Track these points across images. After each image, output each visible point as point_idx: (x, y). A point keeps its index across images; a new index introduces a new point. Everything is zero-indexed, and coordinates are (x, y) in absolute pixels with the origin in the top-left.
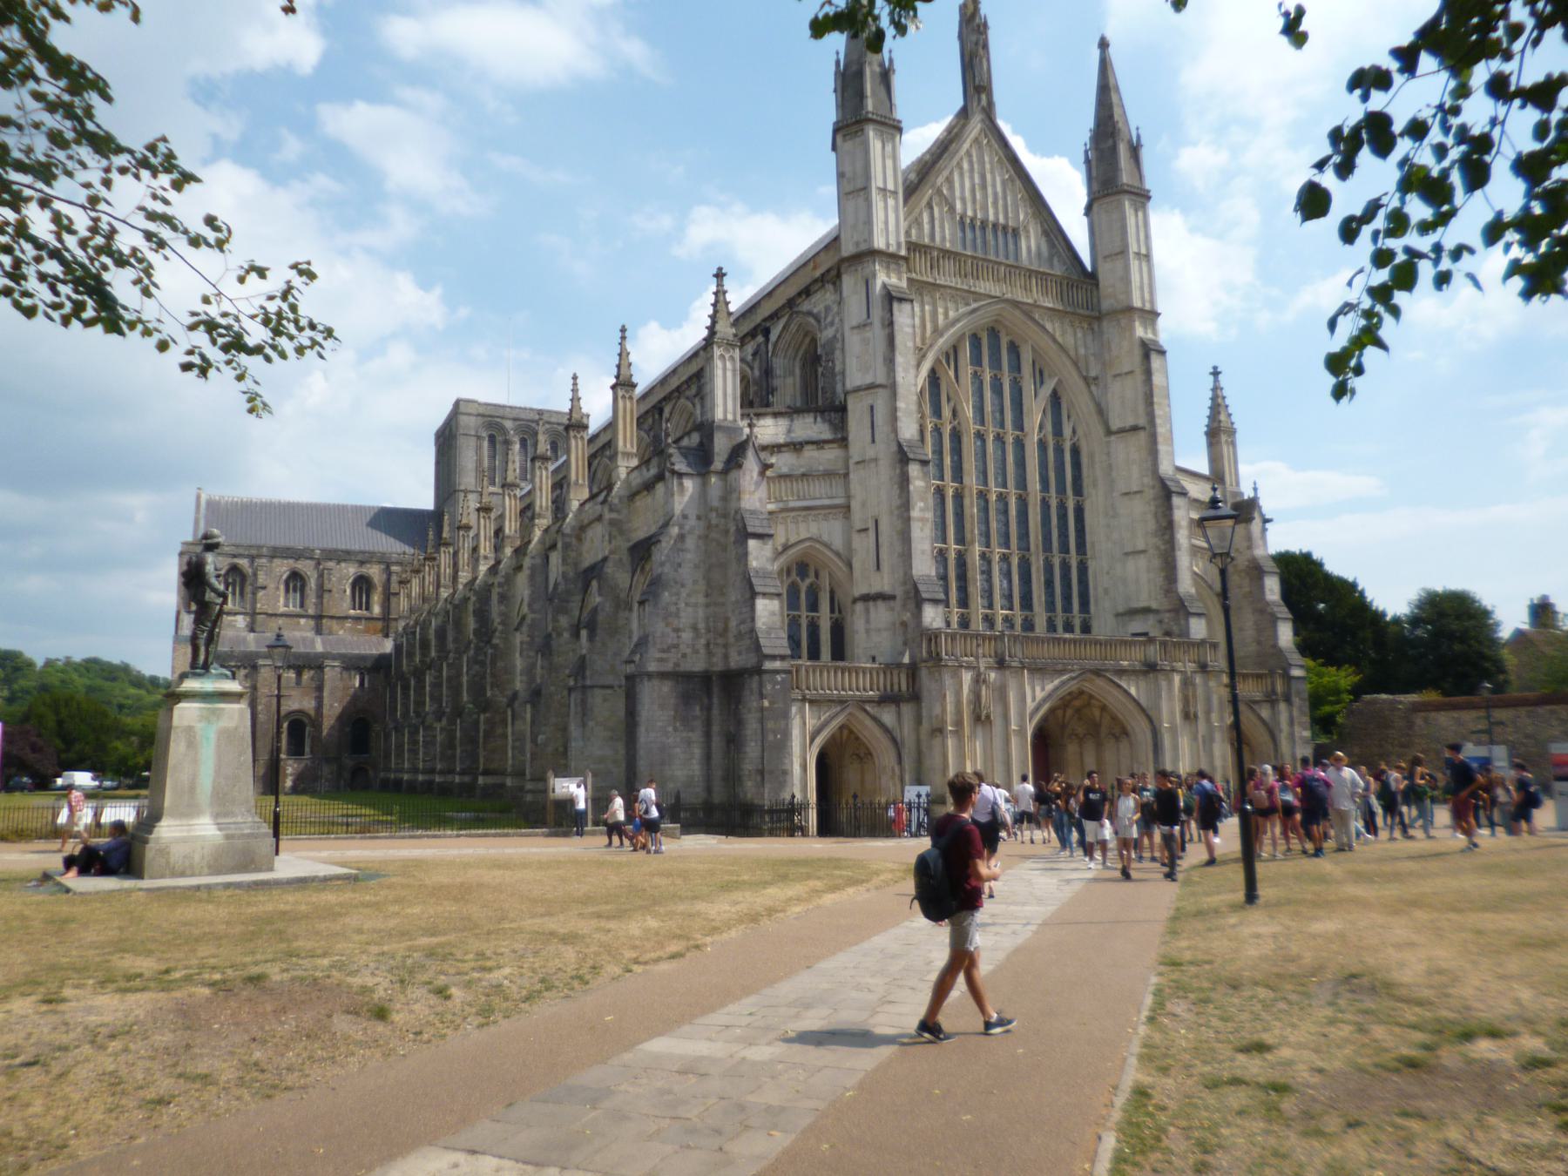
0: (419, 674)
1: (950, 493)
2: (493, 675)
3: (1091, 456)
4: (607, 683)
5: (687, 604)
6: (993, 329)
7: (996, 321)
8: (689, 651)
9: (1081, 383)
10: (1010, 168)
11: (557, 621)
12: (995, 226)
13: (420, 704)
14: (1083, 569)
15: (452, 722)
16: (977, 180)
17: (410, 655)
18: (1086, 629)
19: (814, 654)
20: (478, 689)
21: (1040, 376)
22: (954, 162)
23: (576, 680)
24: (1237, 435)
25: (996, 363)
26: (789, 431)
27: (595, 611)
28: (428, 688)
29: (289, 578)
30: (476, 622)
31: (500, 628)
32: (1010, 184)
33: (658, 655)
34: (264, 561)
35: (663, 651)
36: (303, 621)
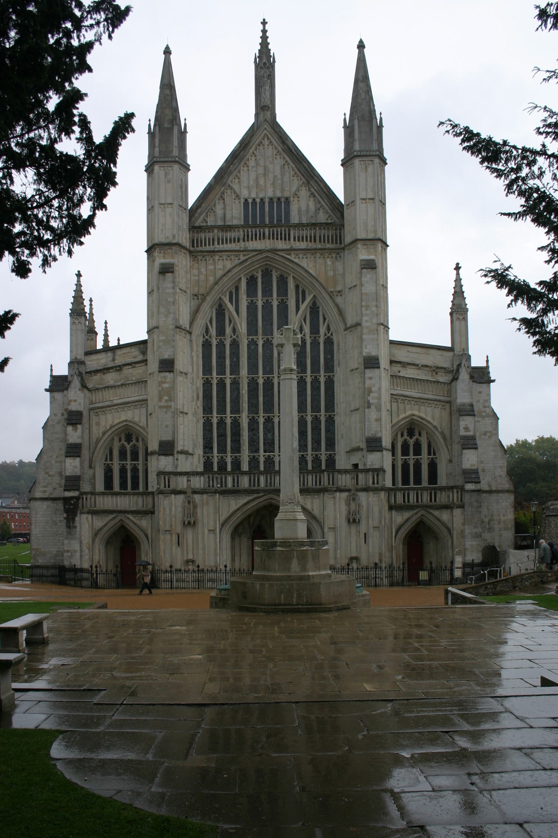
1: (228, 382)
3: (338, 346)
5: (56, 462)
6: (267, 269)
7: (266, 264)
8: (58, 486)
9: (327, 297)
10: (285, 156)
12: (271, 199)
14: (331, 421)
16: (261, 170)
18: (331, 461)
19: (135, 485)
21: (301, 295)
22: (243, 163)
24: (469, 313)
25: (267, 291)
26: (114, 360)
32: (286, 167)
33: (41, 489)
35: (45, 487)
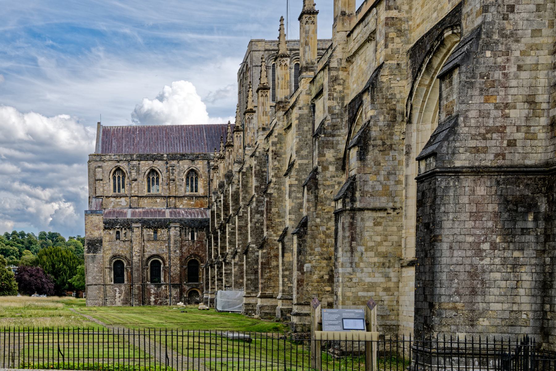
0: (222, 228)
2: (269, 219)
4: (378, 205)
11: (324, 155)
13: (224, 248)
15: (241, 260)
17: (219, 216)
20: (258, 231)
23: (344, 203)
27: (367, 128)
28: (227, 237)
29: (149, 173)
30: (257, 181)
31: (274, 180)
34: (134, 163)
36: (158, 200)
